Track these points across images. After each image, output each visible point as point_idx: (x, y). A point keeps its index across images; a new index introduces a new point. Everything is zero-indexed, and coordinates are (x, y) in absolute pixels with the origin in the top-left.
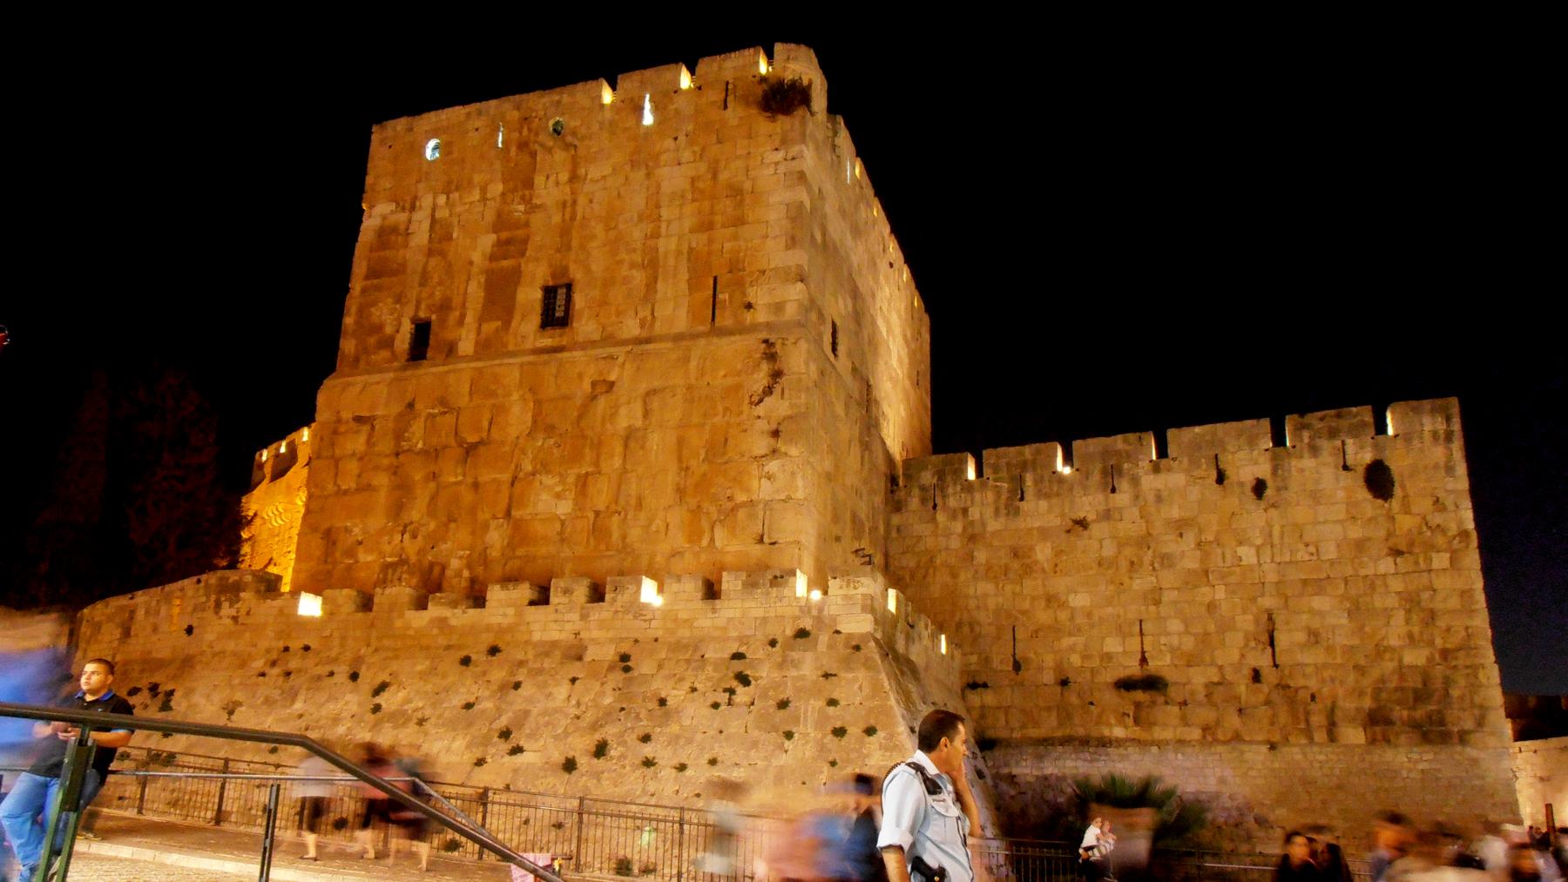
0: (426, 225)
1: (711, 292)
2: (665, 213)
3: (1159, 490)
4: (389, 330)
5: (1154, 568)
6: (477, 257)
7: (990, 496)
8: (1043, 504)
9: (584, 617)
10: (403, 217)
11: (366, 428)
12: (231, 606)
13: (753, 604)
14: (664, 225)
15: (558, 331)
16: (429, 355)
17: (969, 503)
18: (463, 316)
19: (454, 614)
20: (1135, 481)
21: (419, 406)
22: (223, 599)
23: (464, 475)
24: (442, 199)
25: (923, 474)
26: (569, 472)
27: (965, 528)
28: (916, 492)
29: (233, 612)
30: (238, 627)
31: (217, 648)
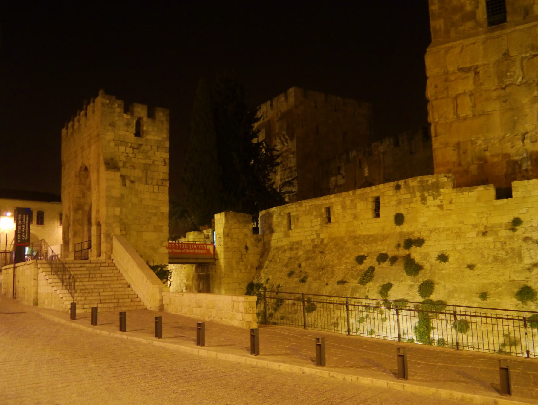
4: (469, 8)
11: (471, 75)
16: (509, 18)
22: (426, 194)
29: (438, 202)
30: (444, 212)
31: (431, 226)
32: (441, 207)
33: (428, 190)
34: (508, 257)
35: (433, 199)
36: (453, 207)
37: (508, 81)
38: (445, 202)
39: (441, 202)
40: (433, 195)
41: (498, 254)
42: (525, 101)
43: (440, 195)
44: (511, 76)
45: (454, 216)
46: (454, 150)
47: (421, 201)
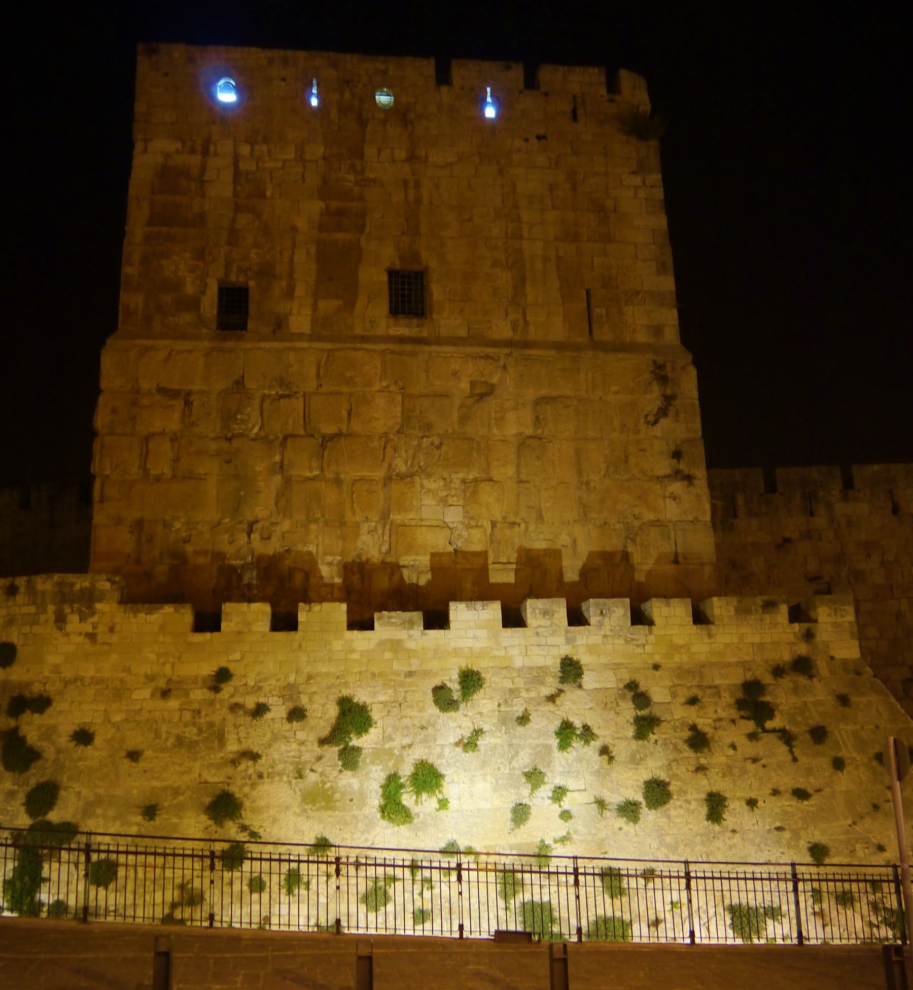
0: (227, 176)
2: (525, 215)
4: (190, 289)
5: (850, 582)
8: (755, 522)
9: (569, 641)
10: (195, 160)
15: (415, 321)
16: (251, 325)
19: (410, 637)
20: (829, 507)
21: (250, 384)
22: (67, 610)
23: (322, 470)
24: (245, 150)
26: (454, 476)
31: (68, 674)
32: (92, 637)
33: (71, 602)
34: (201, 738)
35: (78, 621)
36: (115, 639)
37: (237, 428)
38: (101, 629)
39: (94, 628)
40: (80, 612)
41: (185, 733)
42: (260, 467)
43: (93, 614)
44: (243, 422)
45: (114, 657)
46: (131, 533)
47: (56, 621)
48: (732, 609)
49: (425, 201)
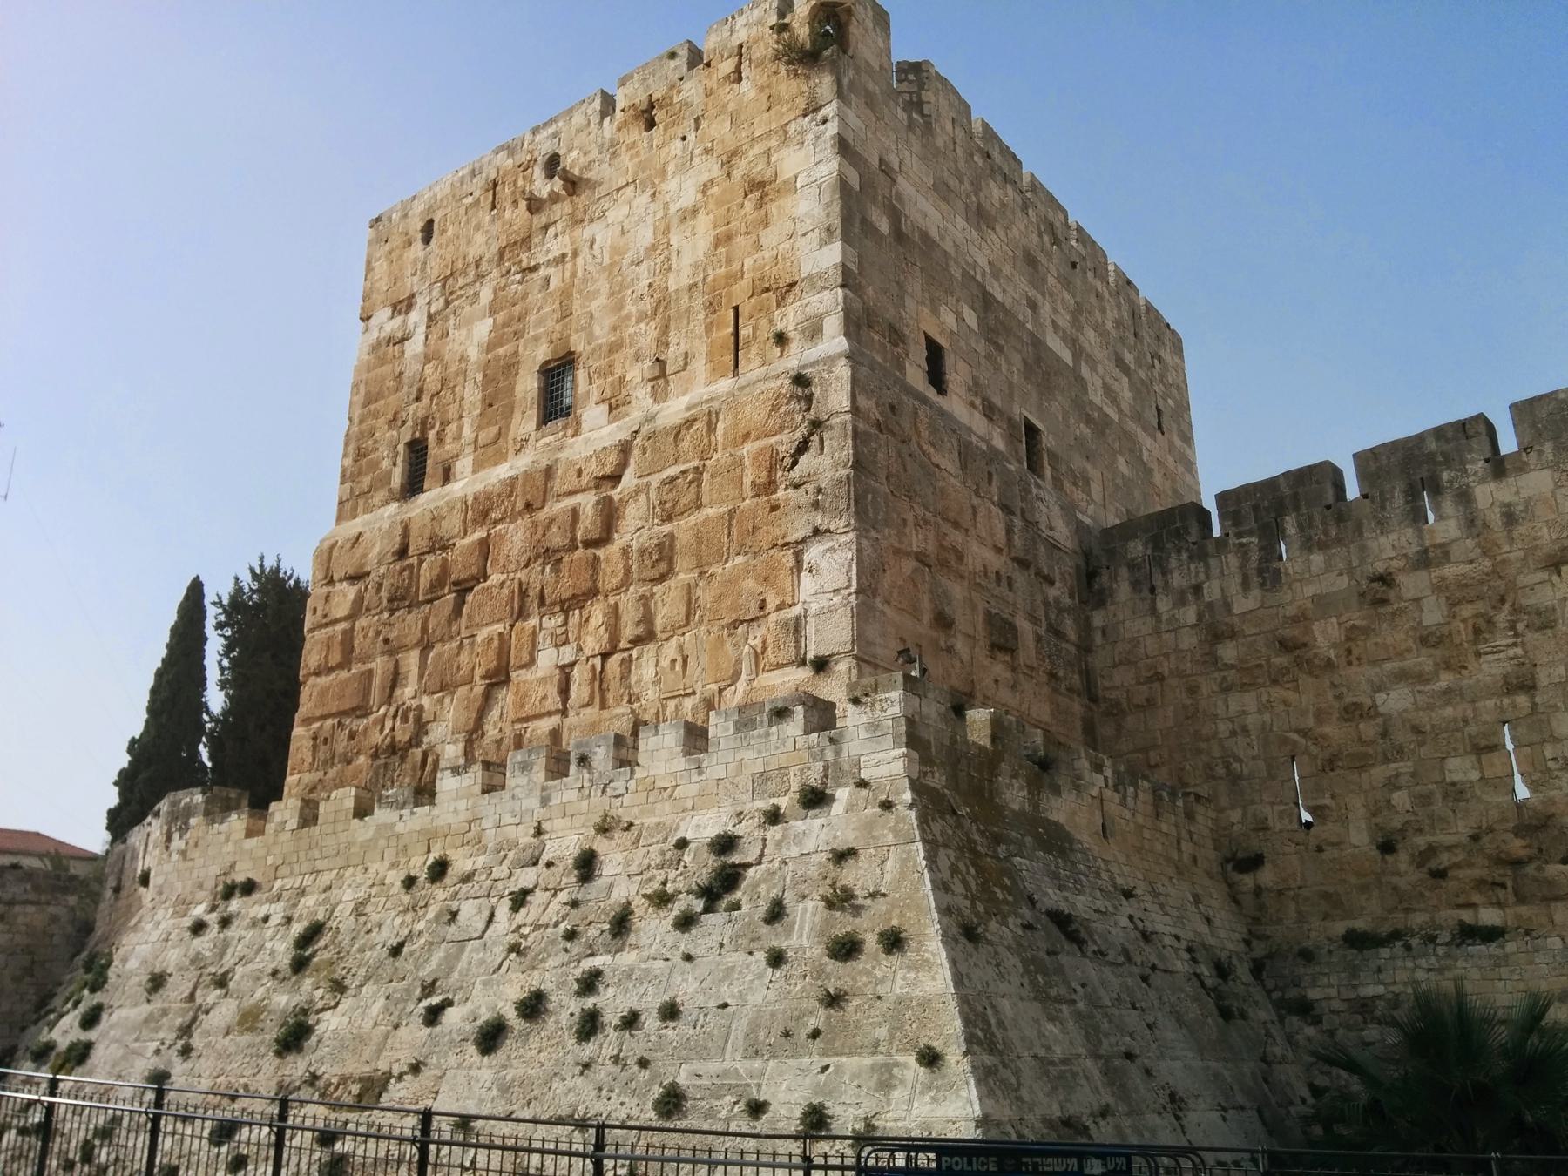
1: (731, 330)
2: (674, 240)
3: (1509, 505)
4: (385, 464)
6: (474, 354)
7: (1233, 561)
8: (1317, 559)
12: (181, 837)
13: (748, 754)
14: (674, 257)
17: (1202, 576)
18: (460, 428)
20: (1464, 497)
25: (1132, 544)
27: (1200, 616)
28: (1124, 572)
48: (731, 724)
49: (580, 274)
